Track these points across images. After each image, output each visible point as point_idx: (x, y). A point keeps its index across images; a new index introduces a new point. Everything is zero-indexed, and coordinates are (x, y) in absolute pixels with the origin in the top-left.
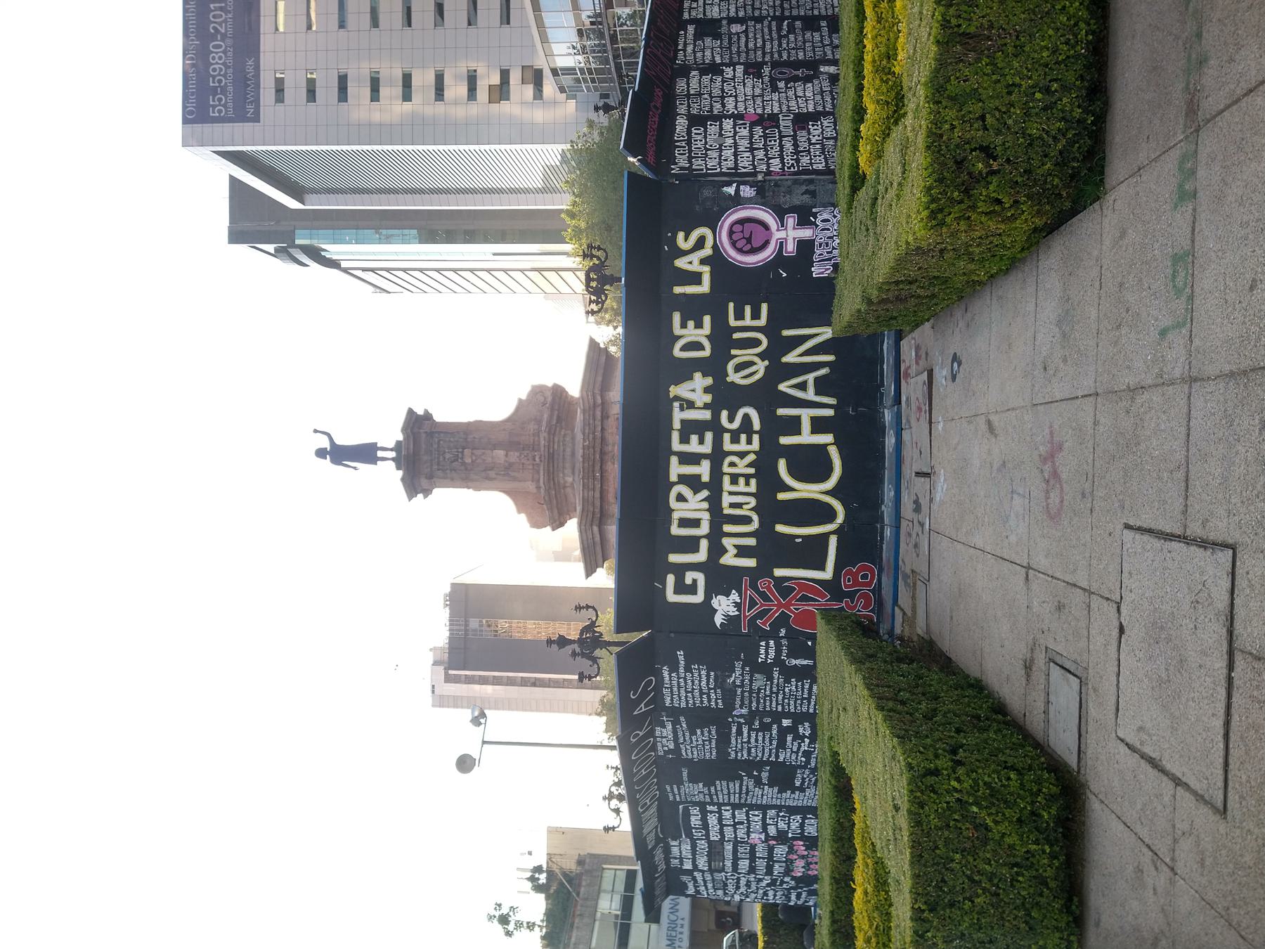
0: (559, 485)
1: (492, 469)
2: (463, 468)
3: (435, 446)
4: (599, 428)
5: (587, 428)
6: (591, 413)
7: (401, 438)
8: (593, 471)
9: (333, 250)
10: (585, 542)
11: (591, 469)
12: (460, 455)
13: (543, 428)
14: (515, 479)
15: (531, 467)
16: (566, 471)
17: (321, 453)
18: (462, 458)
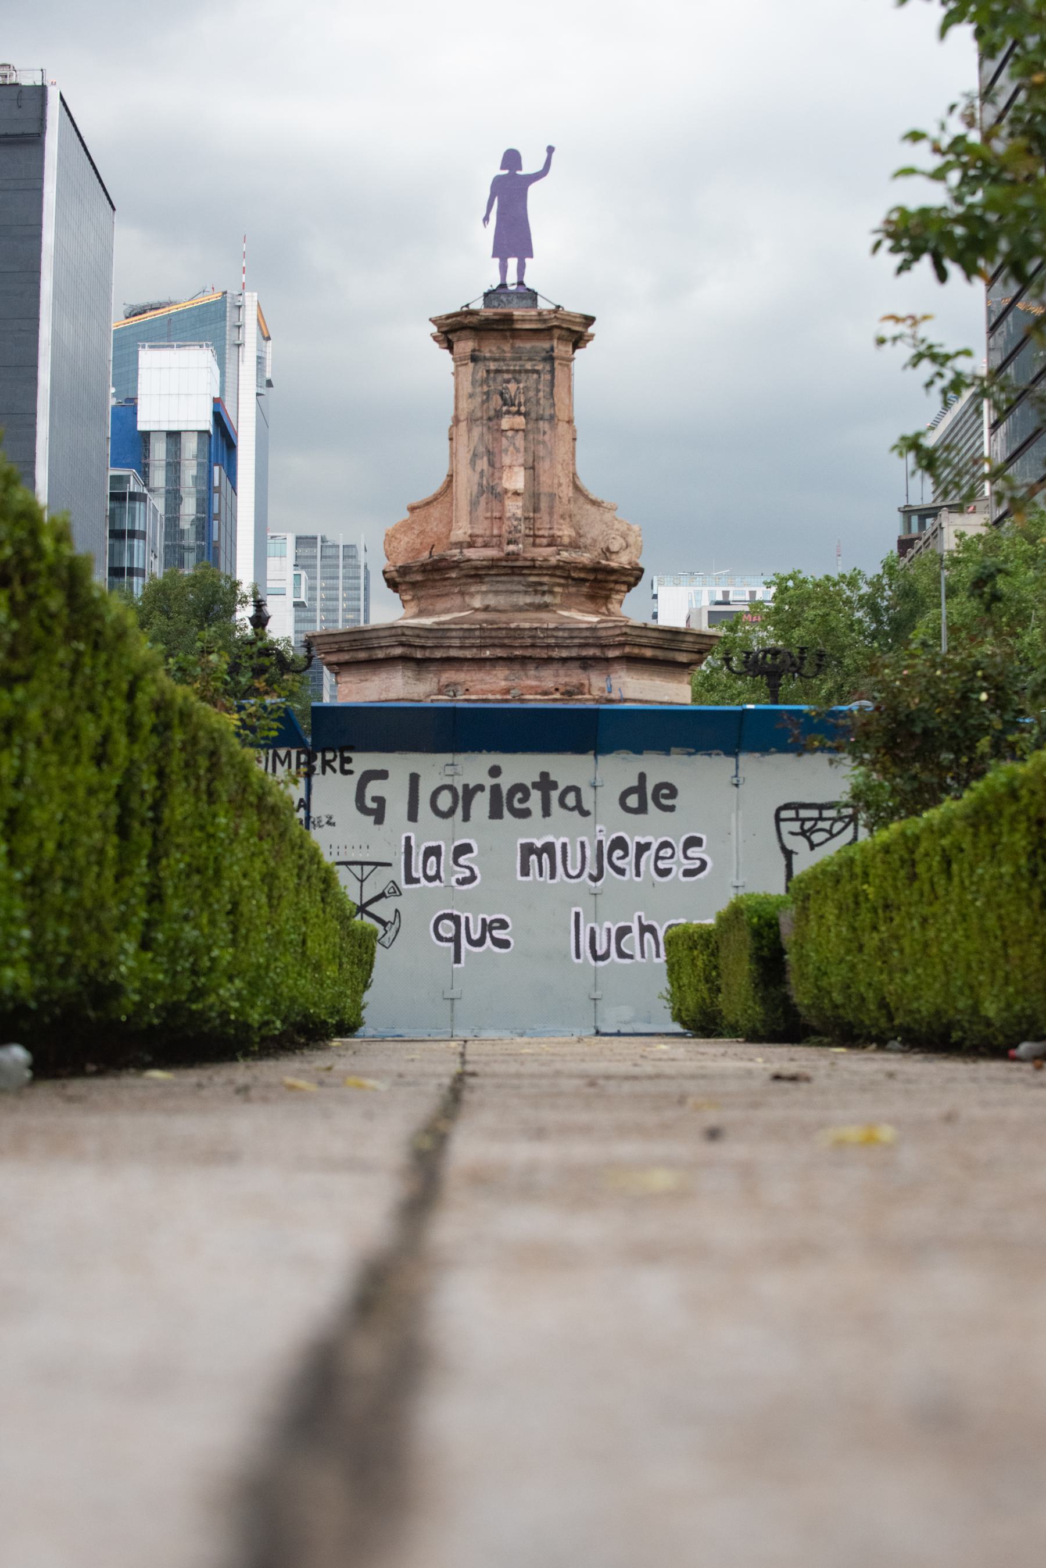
0: (465, 584)
1: (491, 464)
2: (492, 413)
4: (565, 654)
5: (566, 635)
6: (591, 641)
7: (543, 305)
8: (494, 646)
10: (374, 634)
11: (496, 641)
12: (514, 409)
13: (565, 555)
14: (474, 504)
15: (496, 532)
16: (490, 596)
17: (512, 159)
18: (508, 412)
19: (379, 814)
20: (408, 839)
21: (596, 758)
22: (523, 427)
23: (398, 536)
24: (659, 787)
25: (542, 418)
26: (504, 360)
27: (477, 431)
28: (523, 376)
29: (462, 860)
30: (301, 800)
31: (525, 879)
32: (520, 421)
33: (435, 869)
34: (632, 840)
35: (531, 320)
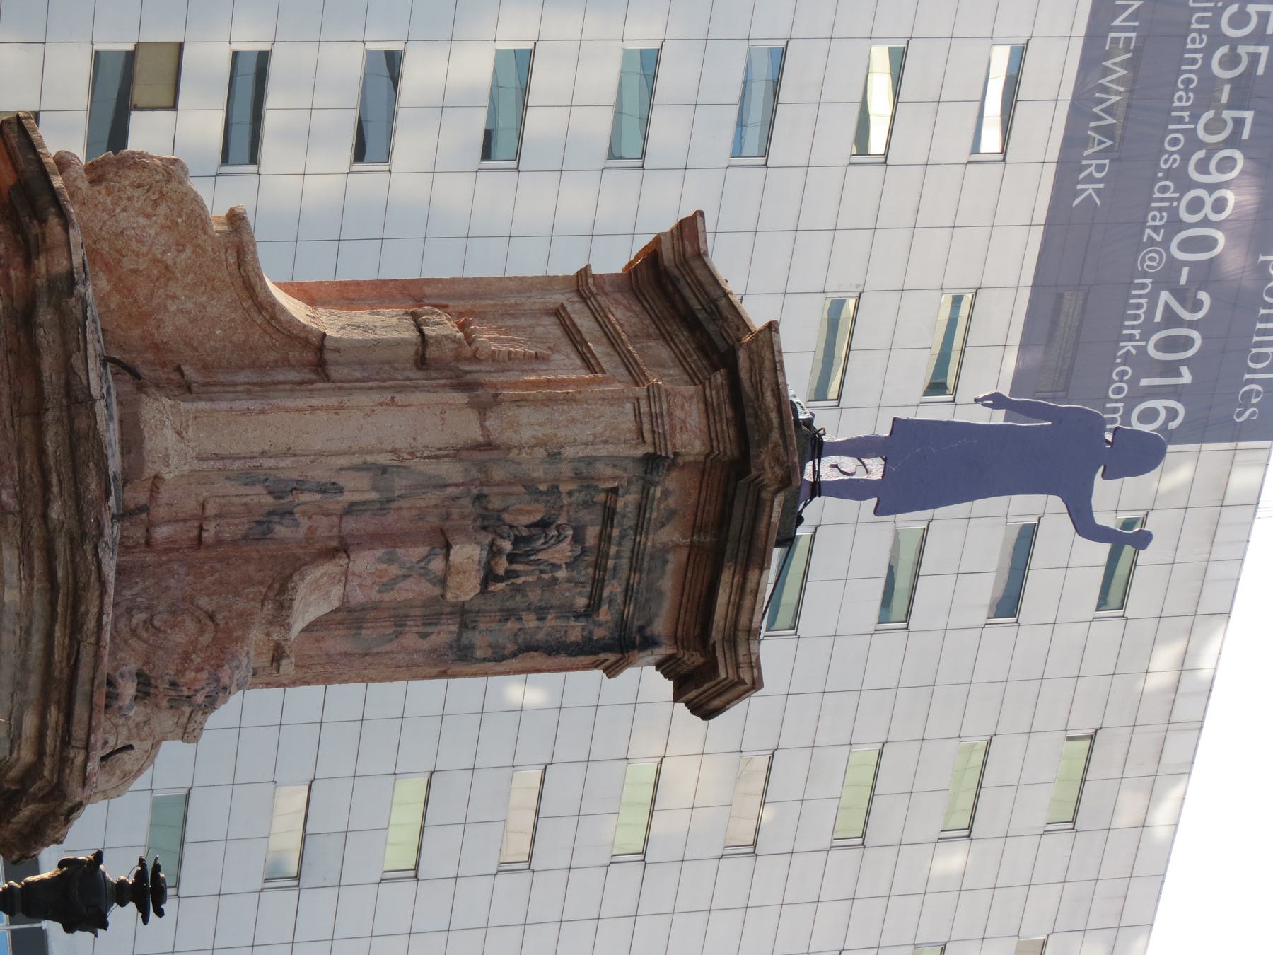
0: (26, 534)
3: (613, 588)
18: (494, 552)
22: (449, 596)
23: (162, 210)
25: (464, 626)
26: (639, 528)
27: (451, 471)
28: (586, 573)
32: (466, 588)
35: (738, 608)
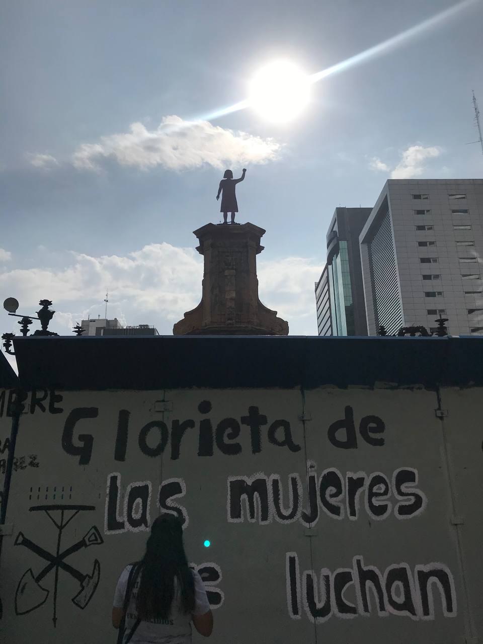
9: (338, 260)
12: (230, 267)
19: (85, 455)
20: (114, 479)
21: (303, 393)
24: (365, 421)
29: (169, 502)
30: (7, 440)
31: (236, 521)
33: (141, 511)
34: (344, 475)
